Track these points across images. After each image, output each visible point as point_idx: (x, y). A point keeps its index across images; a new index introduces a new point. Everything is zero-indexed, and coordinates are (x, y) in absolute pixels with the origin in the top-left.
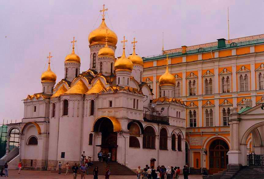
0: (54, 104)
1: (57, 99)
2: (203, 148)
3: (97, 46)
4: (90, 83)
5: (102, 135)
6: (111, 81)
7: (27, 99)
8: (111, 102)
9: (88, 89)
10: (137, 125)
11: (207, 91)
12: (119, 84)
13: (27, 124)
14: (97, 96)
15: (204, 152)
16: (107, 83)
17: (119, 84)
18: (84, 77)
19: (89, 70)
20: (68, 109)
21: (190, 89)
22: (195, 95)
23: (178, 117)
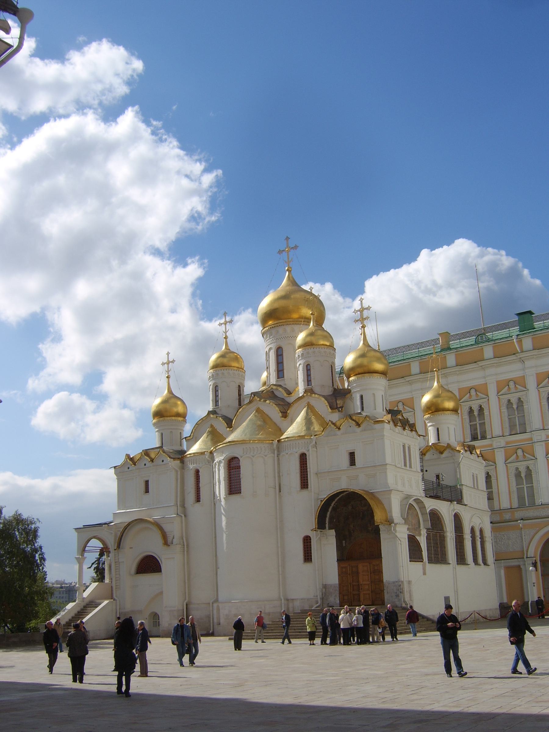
0: (197, 472)
2: (527, 555)
4: (285, 415)
5: (336, 536)
7: (123, 465)
8: (352, 455)
9: (280, 429)
10: (412, 505)
11: (512, 426)
12: (362, 409)
13: (129, 524)
15: (533, 563)
16: (330, 410)
17: (362, 409)
18: (268, 402)
19: (274, 387)
20: (240, 479)
21: (470, 425)
22: (486, 437)
23: (476, 488)
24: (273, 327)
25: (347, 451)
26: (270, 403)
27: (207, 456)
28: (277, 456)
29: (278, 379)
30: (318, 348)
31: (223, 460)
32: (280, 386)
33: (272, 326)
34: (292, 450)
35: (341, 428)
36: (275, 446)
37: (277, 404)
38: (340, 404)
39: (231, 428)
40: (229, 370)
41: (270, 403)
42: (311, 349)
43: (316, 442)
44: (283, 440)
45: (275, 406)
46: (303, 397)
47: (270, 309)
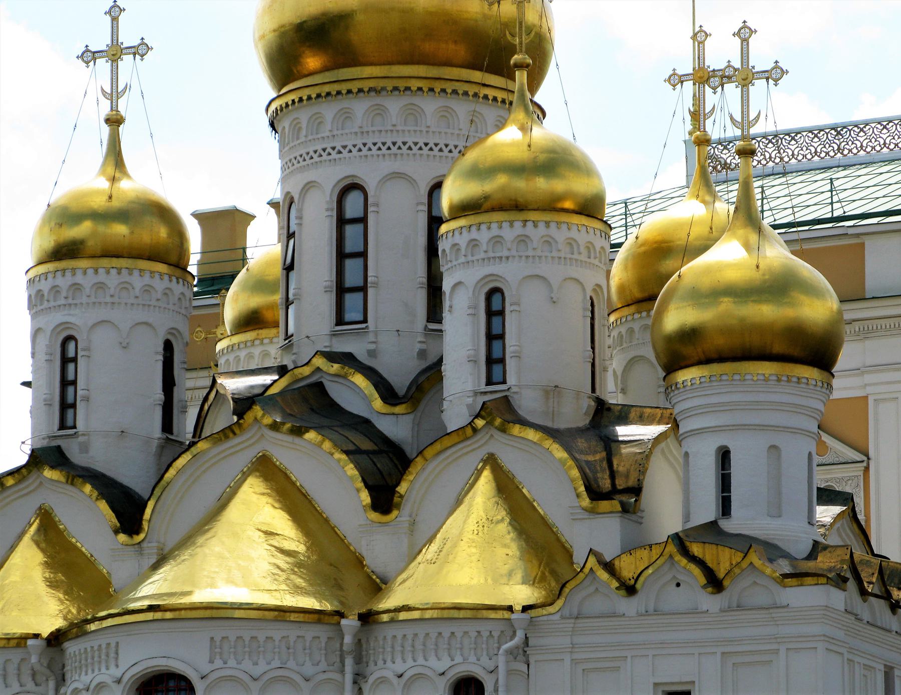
1: (15, 656)
3: (381, 111)
6: (621, 484)
14: (520, 635)
16: (586, 502)
18: (311, 435)
24: (328, 94)
25: (656, 685)
26: (319, 446)
27: (35, 652)
28: (355, 682)
29: (337, 324)
30: (541, 225)
31: (119, 681)
32: (347, 359)
33: (327, 89)
34: (421, 661)
35: (638, 586)
36: (348, 639)
37: (351, 447)
38: (627, 476)
39: (138, 533)
40: (130, 271)
41: (319, 446)
42: (511, 226)
43: (527, 638)
44: (385, 617)
45: (344, 457)
46: (469, 431)
47: (324, 14)
